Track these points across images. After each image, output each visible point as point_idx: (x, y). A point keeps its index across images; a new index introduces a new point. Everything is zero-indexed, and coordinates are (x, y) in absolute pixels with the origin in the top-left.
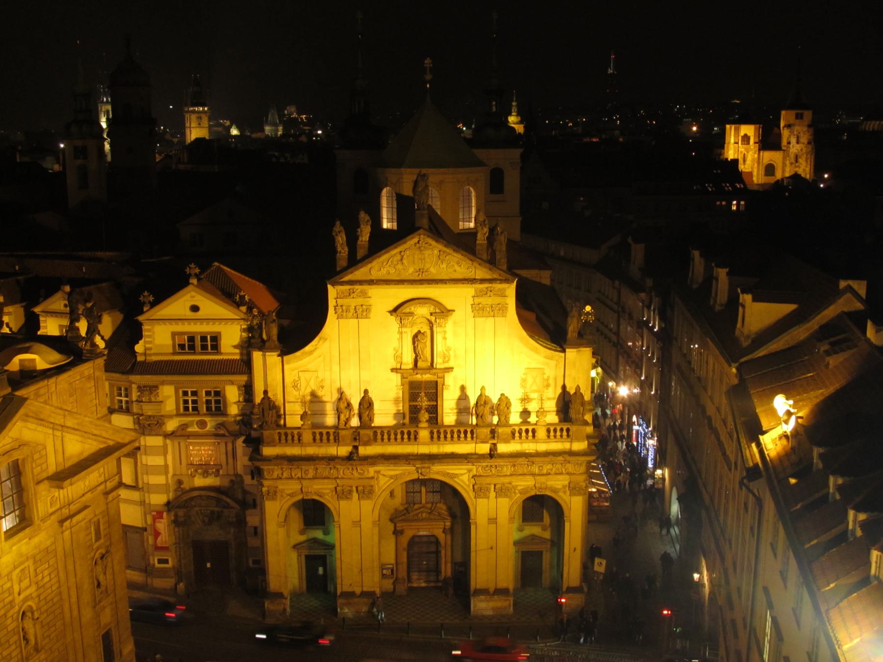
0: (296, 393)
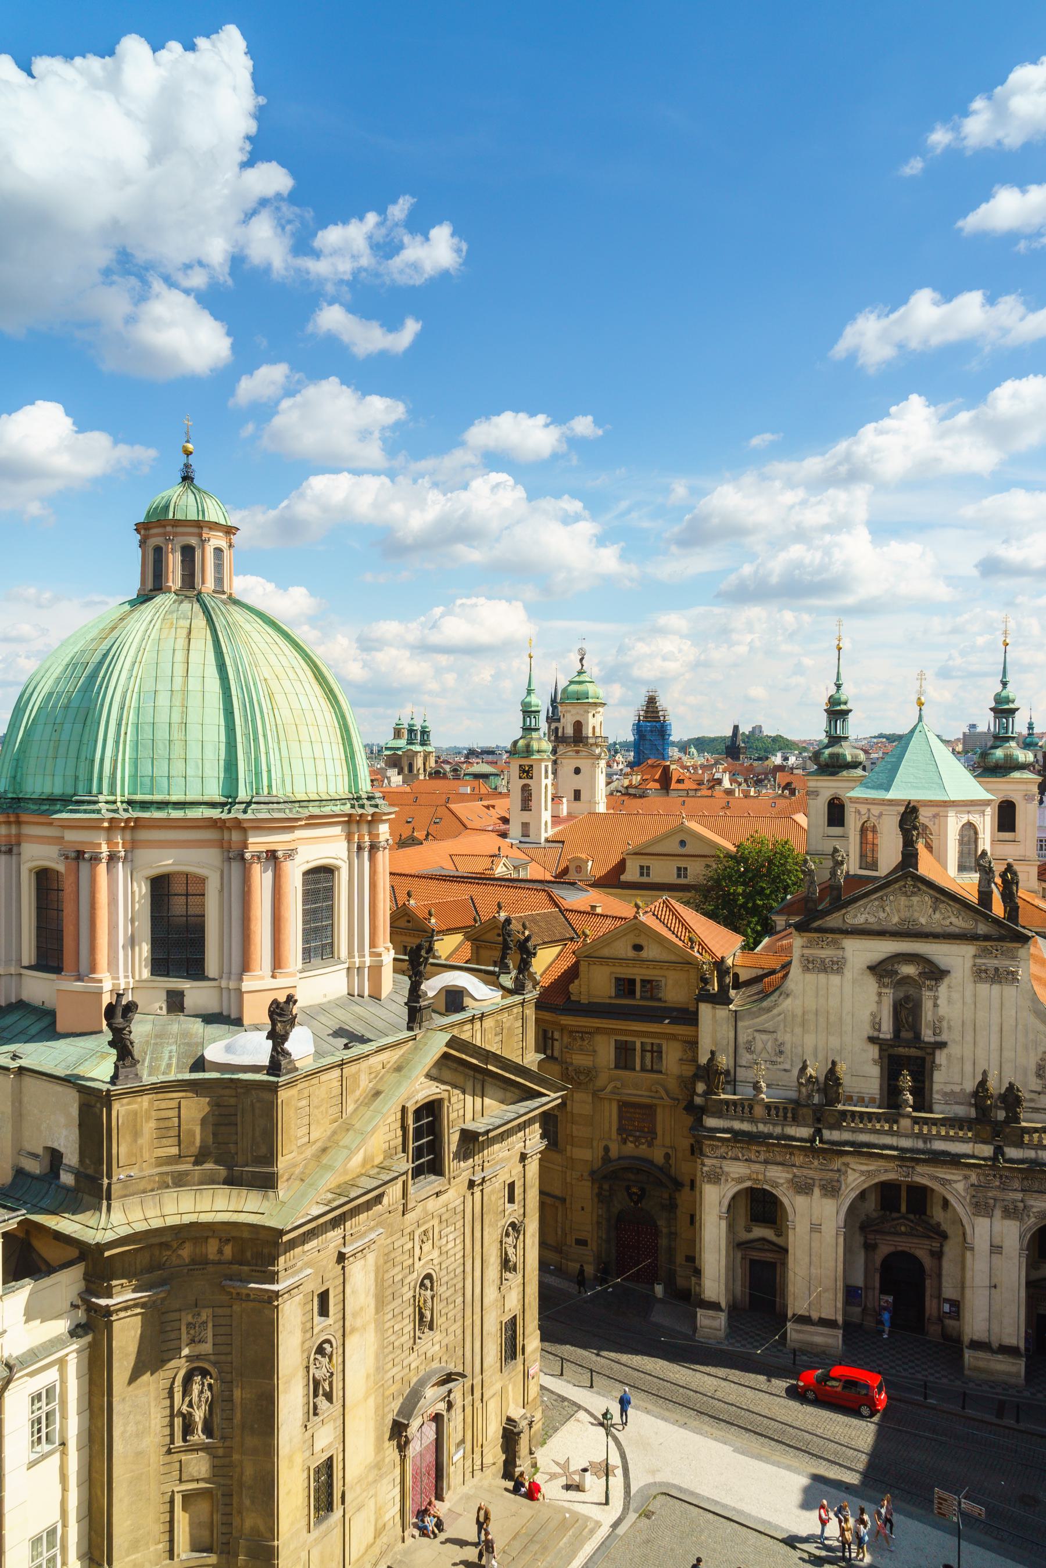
0: (749, 1056)
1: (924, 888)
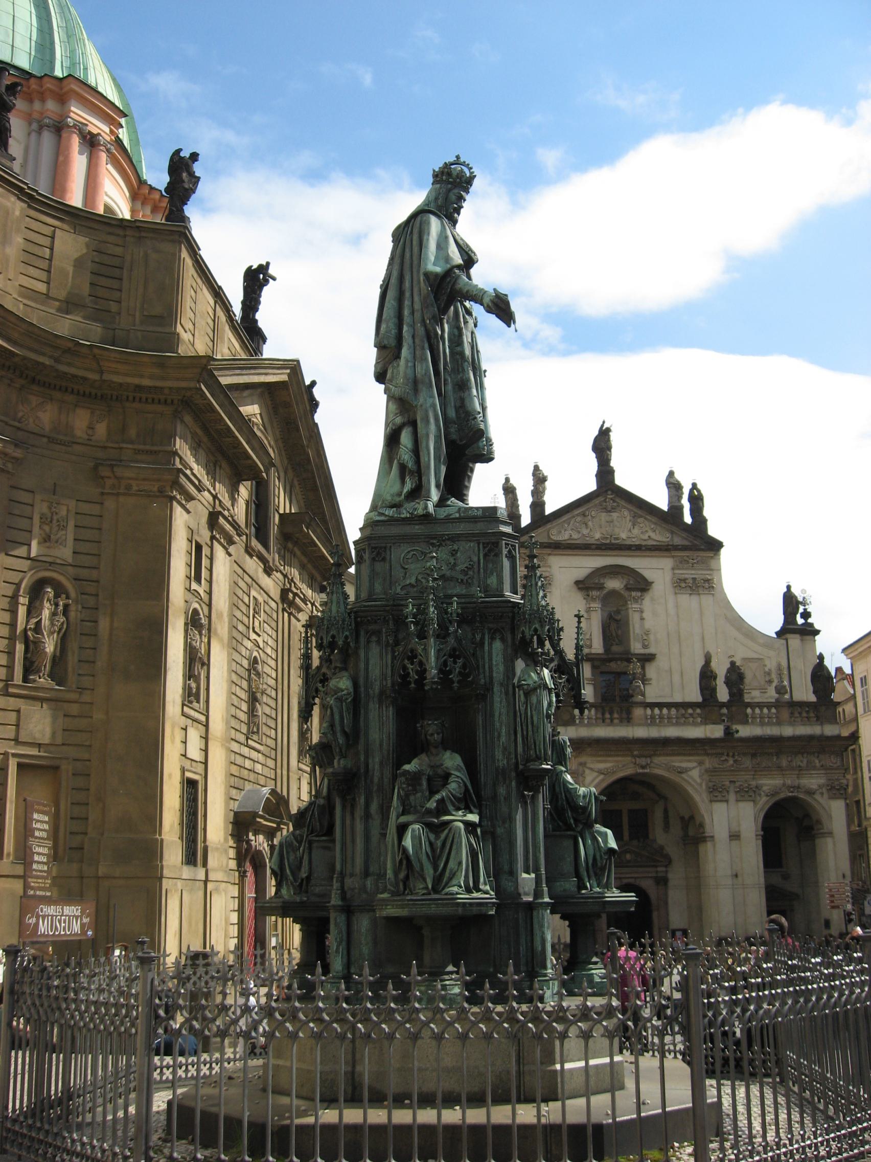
1: (623, 503)
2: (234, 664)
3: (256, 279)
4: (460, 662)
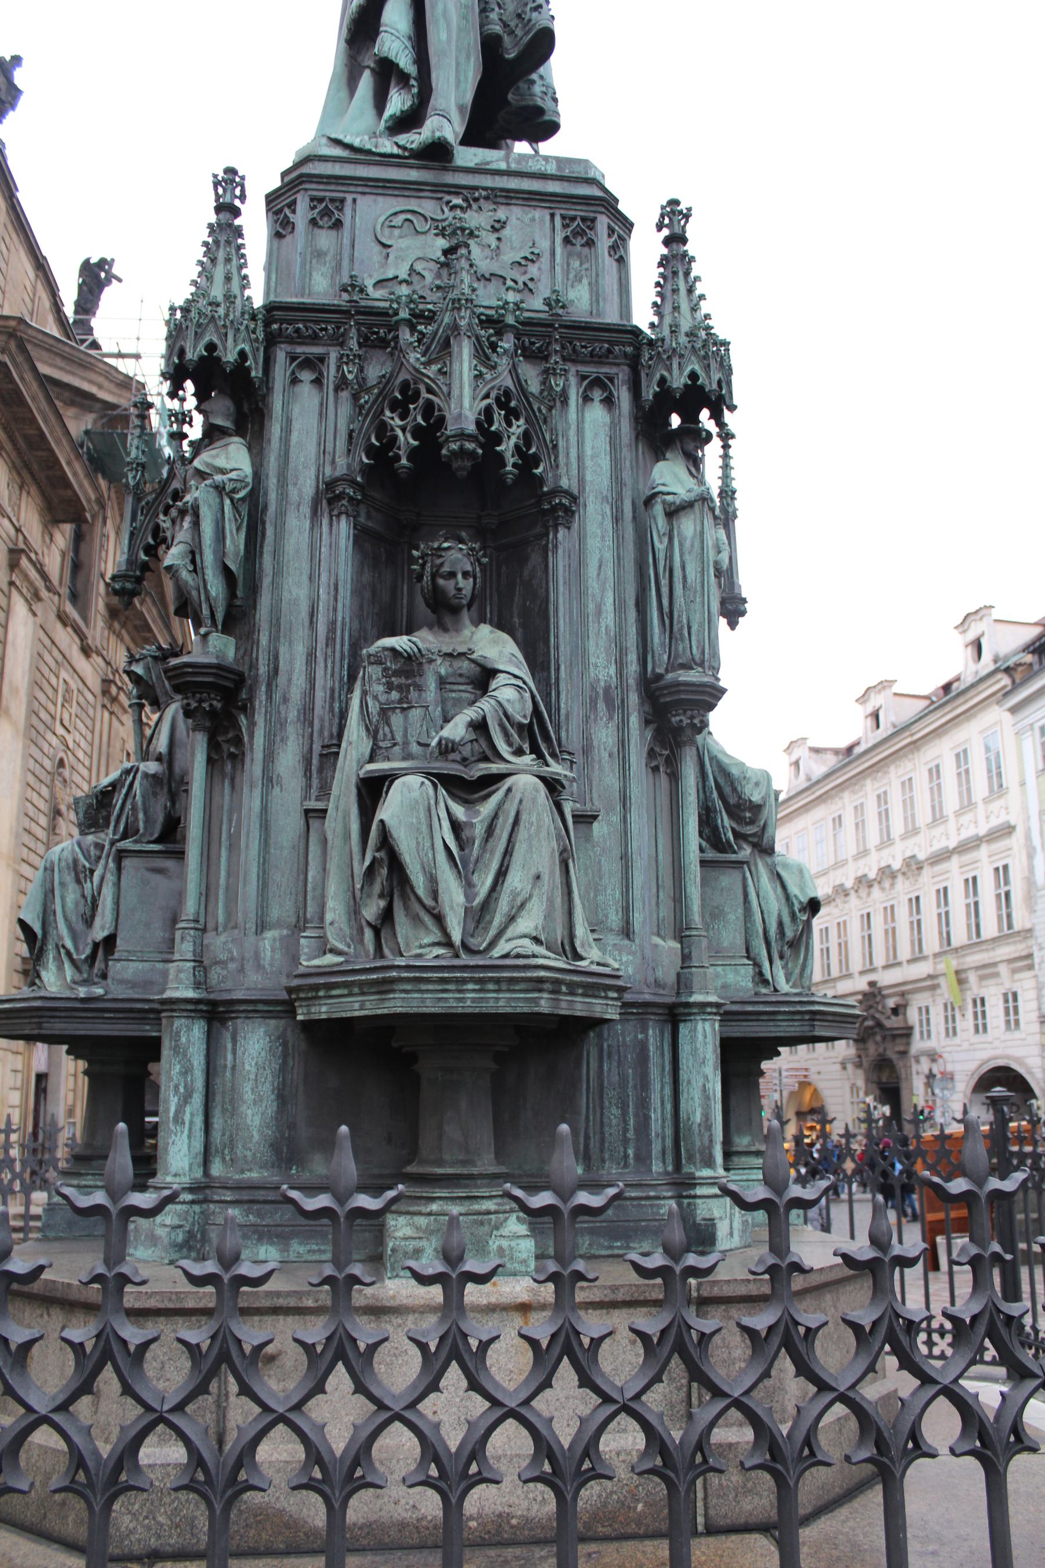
2: (32, 761)
3: (95, 277)
4: (518, 427)
